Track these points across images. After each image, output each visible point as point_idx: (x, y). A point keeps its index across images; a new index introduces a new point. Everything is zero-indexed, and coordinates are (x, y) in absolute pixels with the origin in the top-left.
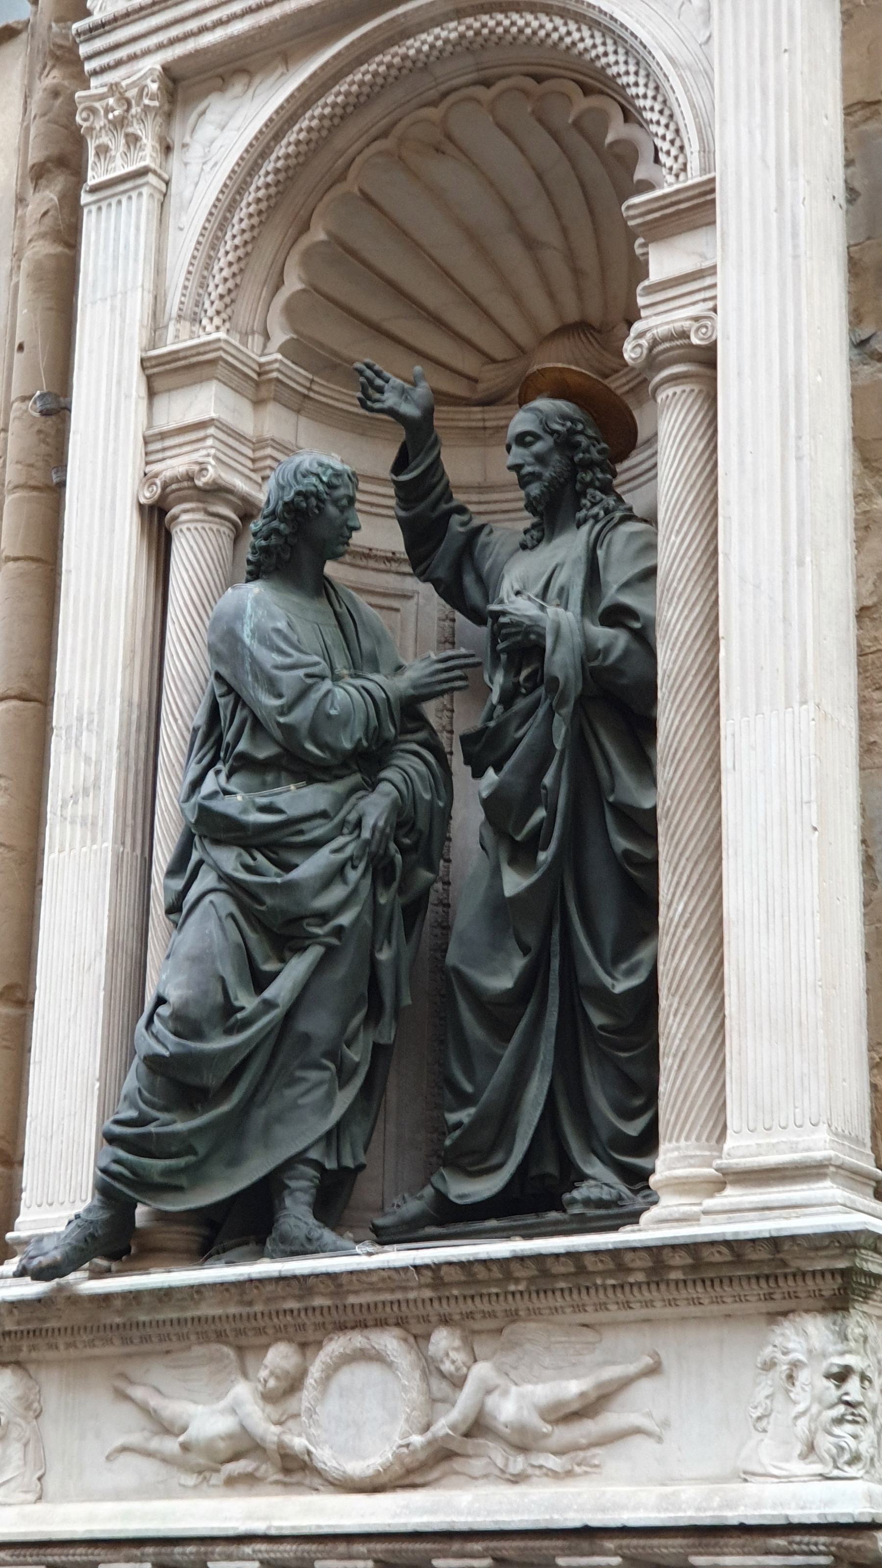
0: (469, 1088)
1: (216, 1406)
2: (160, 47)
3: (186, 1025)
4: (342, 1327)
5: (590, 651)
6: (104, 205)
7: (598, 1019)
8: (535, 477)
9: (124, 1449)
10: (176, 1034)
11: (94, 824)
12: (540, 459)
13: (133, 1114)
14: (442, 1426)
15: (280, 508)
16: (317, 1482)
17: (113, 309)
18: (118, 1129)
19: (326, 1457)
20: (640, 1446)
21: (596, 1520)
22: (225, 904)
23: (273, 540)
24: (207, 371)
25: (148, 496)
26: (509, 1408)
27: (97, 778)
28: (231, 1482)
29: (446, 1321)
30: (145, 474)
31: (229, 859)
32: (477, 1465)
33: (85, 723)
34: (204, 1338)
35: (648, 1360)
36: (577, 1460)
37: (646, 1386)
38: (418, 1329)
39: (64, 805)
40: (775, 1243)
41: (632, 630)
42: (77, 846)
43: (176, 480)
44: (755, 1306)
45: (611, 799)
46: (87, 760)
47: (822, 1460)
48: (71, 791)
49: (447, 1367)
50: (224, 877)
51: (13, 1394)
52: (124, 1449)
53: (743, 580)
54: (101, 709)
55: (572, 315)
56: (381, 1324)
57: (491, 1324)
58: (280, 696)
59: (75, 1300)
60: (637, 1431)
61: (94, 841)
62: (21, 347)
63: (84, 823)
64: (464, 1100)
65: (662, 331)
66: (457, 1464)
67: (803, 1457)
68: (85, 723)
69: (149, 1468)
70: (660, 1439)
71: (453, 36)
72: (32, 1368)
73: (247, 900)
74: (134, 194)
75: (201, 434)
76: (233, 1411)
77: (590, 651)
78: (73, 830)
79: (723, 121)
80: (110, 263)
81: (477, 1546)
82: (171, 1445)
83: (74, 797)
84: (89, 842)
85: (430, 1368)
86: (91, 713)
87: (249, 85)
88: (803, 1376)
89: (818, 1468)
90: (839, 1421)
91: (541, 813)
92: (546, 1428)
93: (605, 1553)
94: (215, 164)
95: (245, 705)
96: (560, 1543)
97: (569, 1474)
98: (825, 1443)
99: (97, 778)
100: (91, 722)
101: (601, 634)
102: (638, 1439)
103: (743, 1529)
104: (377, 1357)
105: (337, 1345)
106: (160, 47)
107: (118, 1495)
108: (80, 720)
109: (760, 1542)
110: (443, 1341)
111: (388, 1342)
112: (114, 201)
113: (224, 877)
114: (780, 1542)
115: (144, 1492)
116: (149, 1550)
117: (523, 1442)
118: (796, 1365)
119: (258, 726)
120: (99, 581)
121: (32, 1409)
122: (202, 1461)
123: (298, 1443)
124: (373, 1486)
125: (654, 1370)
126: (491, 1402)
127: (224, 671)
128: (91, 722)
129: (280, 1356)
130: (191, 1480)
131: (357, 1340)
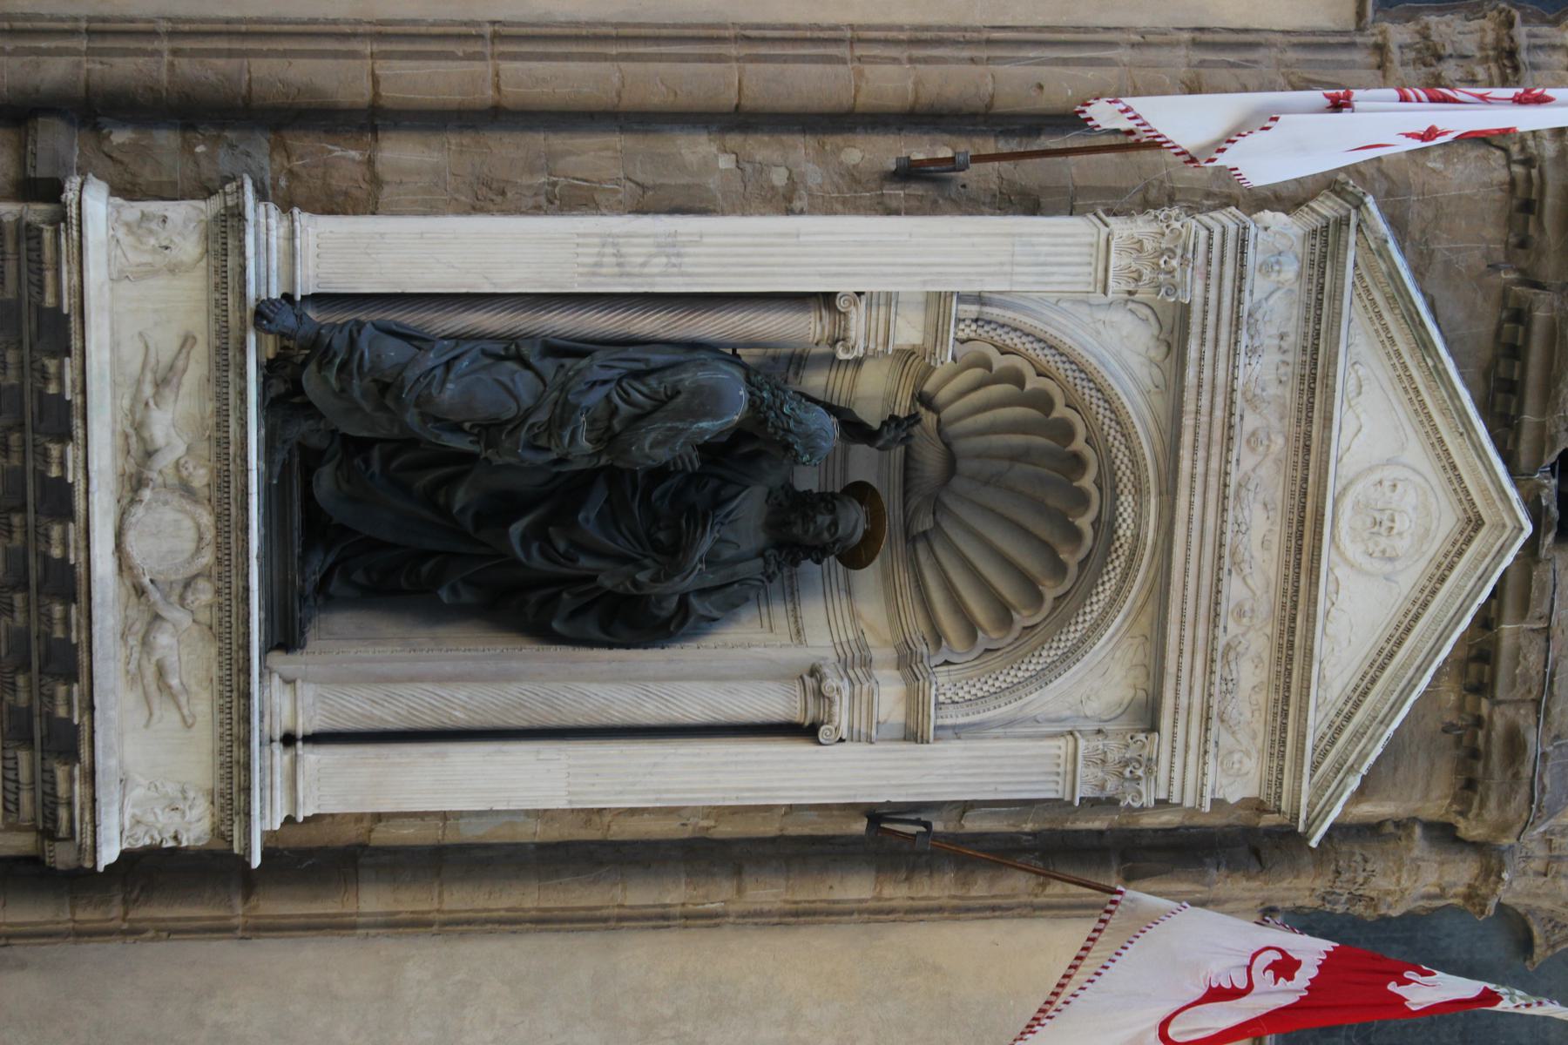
0: (394, 465)
1: (175, 426)
2: (1206, 302)
3: (422, 402)
4: (218, 517)
5: (661, 599)
6: (1094, 251)
7: (425, 569)
8: (806, 532)
9: (147, 348)
10: (418, 397)
11: (594, 274)
12: (818, 534)
13: (367, 365)
14: (155, 596)
15: (790, 439)
16: (125, 501)
17: (1002, 264)
18: (357, 356)
19: (139, 512)
20: (140, 716)
21: (97, 714)
22: (511, 411)
23: (771, 430)
24: (931, 340)
25: (841, 304)
26: (164, 639)
27: (629, 275)
28: (127, 437)
29: (218, 592)
30: (859, 294)
31: (542, 416)
32: (133, 613)
33: (674, 260)
34: (218, 412)
35: (190, 721)
36: (135, 678)
37: (177, 717)
38: (214, 573)
39: (614, 245)
40: (248, 814)
41: (669, 620)
42: (579, 260)
43: (846, 329)
44: (218, 786)
45: (565, 596)
46: (643, 265)
47: (132, 827)
48: (624, 250)
49: (190, 597)
50: (529, 413)
51: (185, 258)
52: (147, 348)
53: (655, 765)
54: (683, 275)
55: (964, 466)
56: (218, 548)
57: (215, 621)
58: (651, 447)
59: (244, 330)
60: (151, 714)
61: (581, 274)
62: (1040, 87)
63: (596, 265)
64: (387, 459)
65: (836, 709)
66: (134, 599)
67: (133, 816)
68: (674, 260)
69: (136, 366)
70: (147, 725)
71: (1121, 532)
72: (203, 263)
73: (510, 427)
74: (1091, 279)
75: (880, 340)
76: (168, 444)
77: (661, 599)
78: (595, 245)
79: (965, 749)
80: (1042, 259)
81: (84, 636)
82: (148, 390)
83: (618, 255)
84: (581, 270)
85: (188, 584)
86: (680, 265)
87: (1151, 360)
88: (177, 817)
89: (127, 825)
90: (152, 838)
91: (562, 546)
92: (154, 660)
93: (81, 717)
94: (1099, 333)
95: (655, 409)
96: (86, 689)
97: (128, 672)
98: (140, 831)
99: (629, 275)
100: (674, 265)
101: (673, 603)
102: (147, 713)
103: (94, 800)
104: (198, 550)
105: (206, 519)
106: (1206, 302)
107: (115, 346)
108: (678, 255)
109: (88, 806)
110: (204, 594)
111: (207, 558)
112: (1093, 260)
113: (529, 413)
114: (87, 817)
115: (117, 363)
116: (79, 400)
117: (145, 643)
118: (184, 813)
119: (641, 417)
120: (785, 265)
121: (173, 269)
122: (138, 417)
123: (147, 494)
124: (119, 546)
125: (187, 725)
126: (168, 626)
127: (680, 399)
128: (674, 265)
129: (200, 477)
130: (126, 403)
131: (209, 535)
